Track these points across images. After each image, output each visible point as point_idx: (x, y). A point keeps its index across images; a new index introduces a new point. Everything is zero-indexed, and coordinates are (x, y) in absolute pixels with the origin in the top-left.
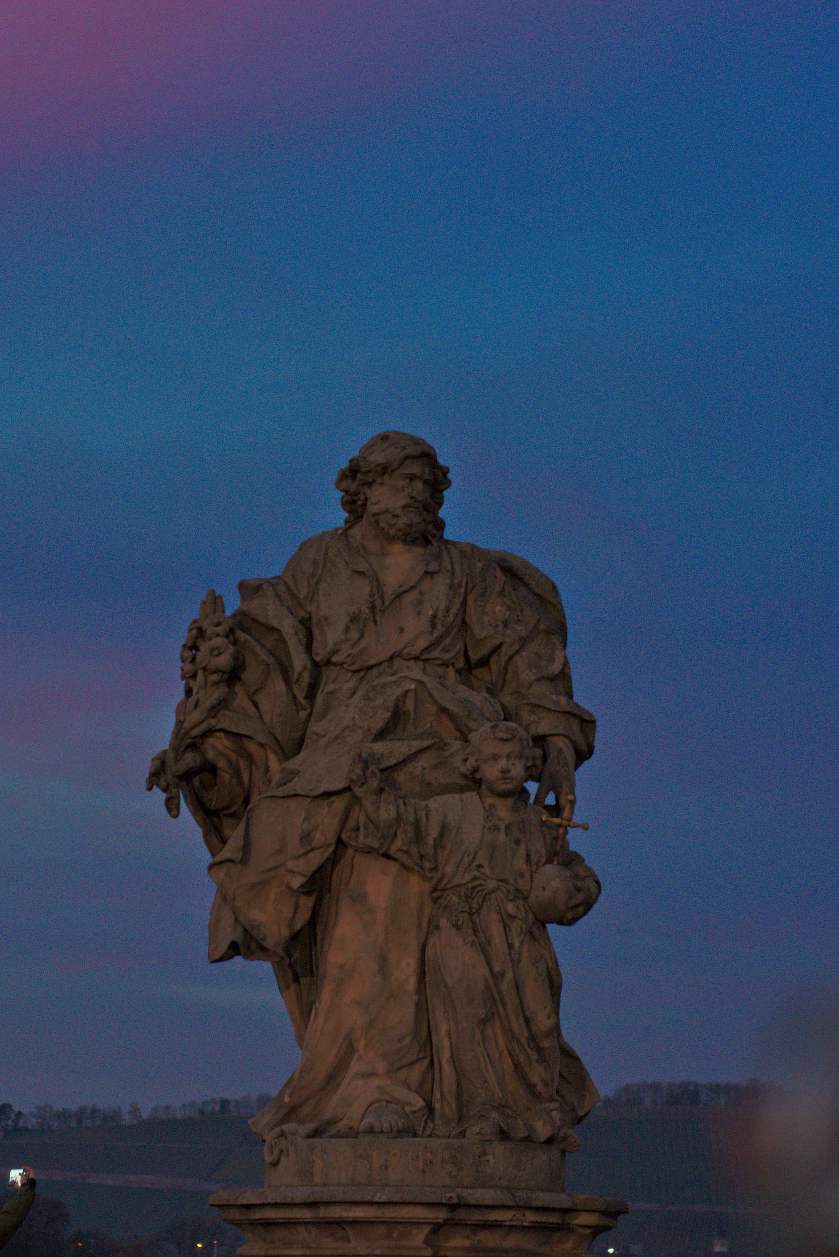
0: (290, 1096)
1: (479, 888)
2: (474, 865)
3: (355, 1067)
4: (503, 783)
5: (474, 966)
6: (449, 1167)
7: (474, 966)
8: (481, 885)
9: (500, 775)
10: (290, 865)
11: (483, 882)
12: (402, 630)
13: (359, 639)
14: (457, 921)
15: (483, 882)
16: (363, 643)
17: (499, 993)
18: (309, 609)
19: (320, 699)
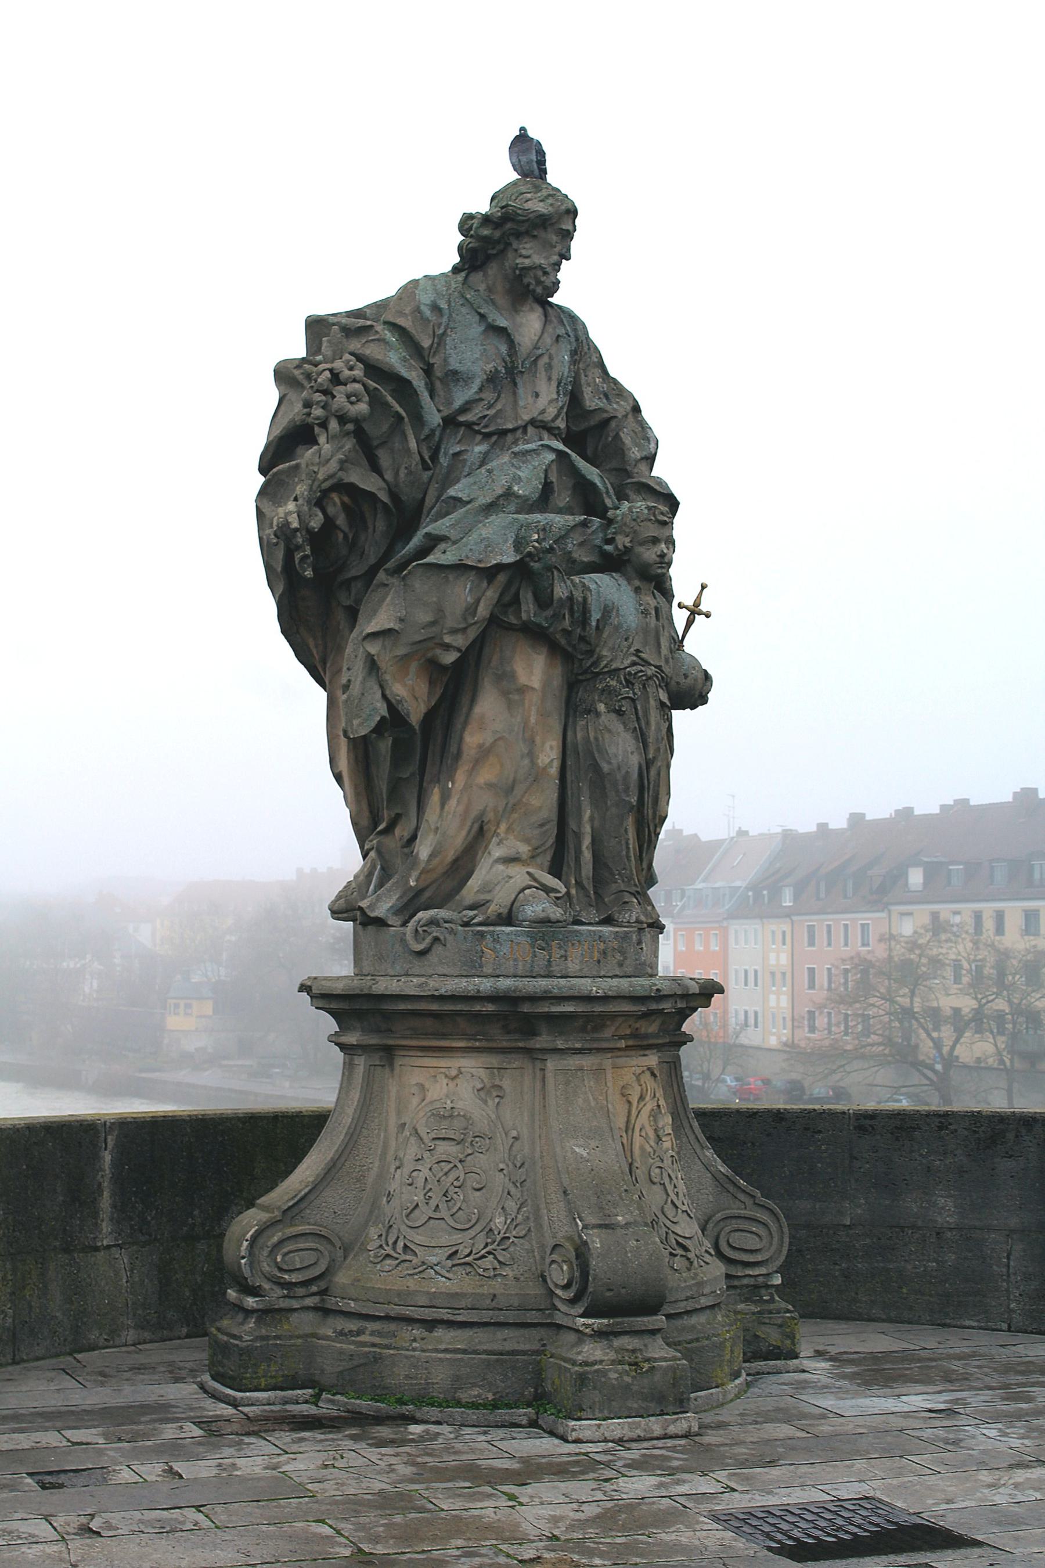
0: (417, 880)
1: (640, 674)
2: (632, 650)
3: (497, 852)
4: (659, 567)
5: (632, 753)
6: (618, 956)
7: (632, 753)
8: (641, 671)
9: (658, 559)
10: (447, 639)
11: (643, 669)
12: (537, 395)
13: (496, 401)
14: (620, 707)
15: (643, 669)
16: (499, 406)
17: (648, 780)
18: (432, 361)
19: (444, 461)
